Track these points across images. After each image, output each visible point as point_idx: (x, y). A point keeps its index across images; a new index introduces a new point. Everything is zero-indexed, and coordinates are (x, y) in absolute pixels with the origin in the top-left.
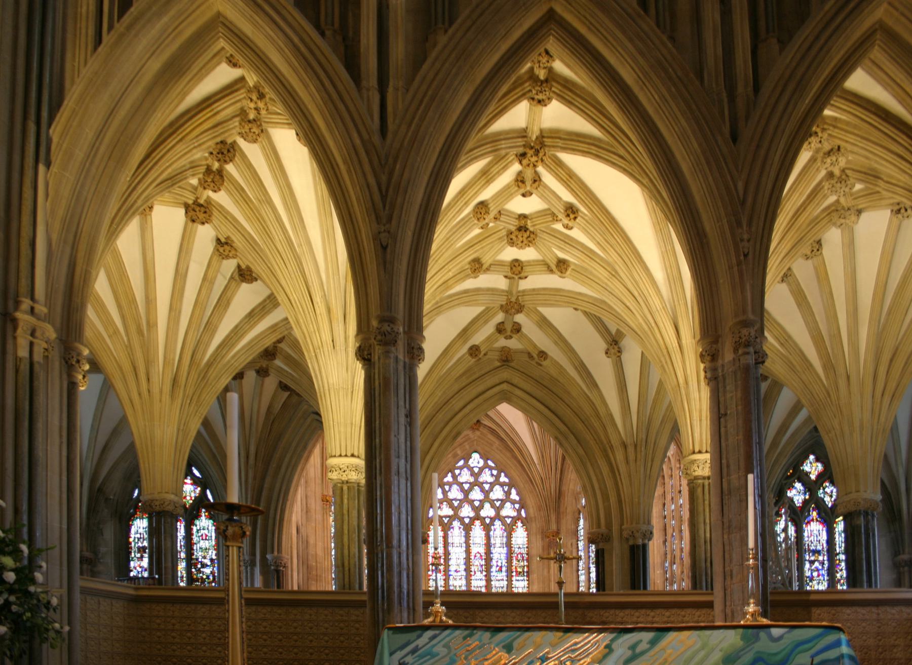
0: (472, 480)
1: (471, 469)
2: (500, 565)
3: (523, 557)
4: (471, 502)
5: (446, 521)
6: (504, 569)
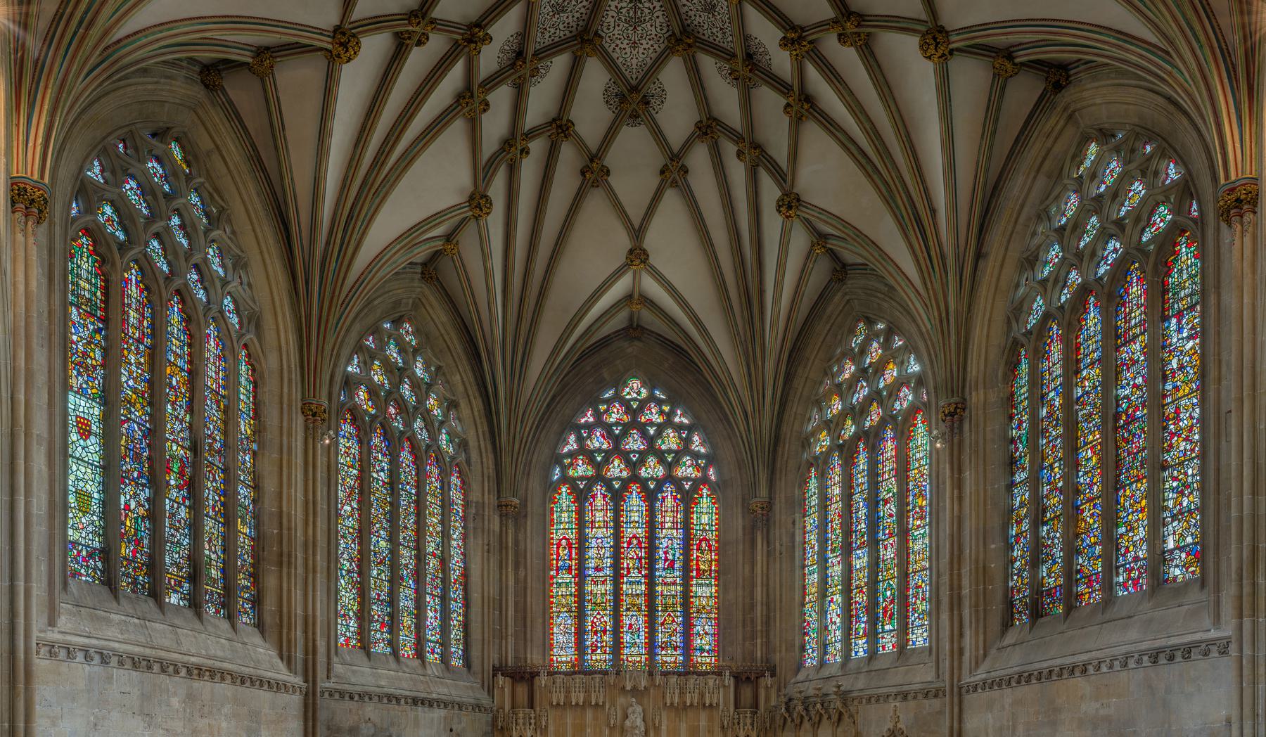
0: (626, 419)
1: (626, 404)
2: (670, 557)
3: (710, 546)
4: (624, 455)
5: (582, 487)
6: (677, 565)
